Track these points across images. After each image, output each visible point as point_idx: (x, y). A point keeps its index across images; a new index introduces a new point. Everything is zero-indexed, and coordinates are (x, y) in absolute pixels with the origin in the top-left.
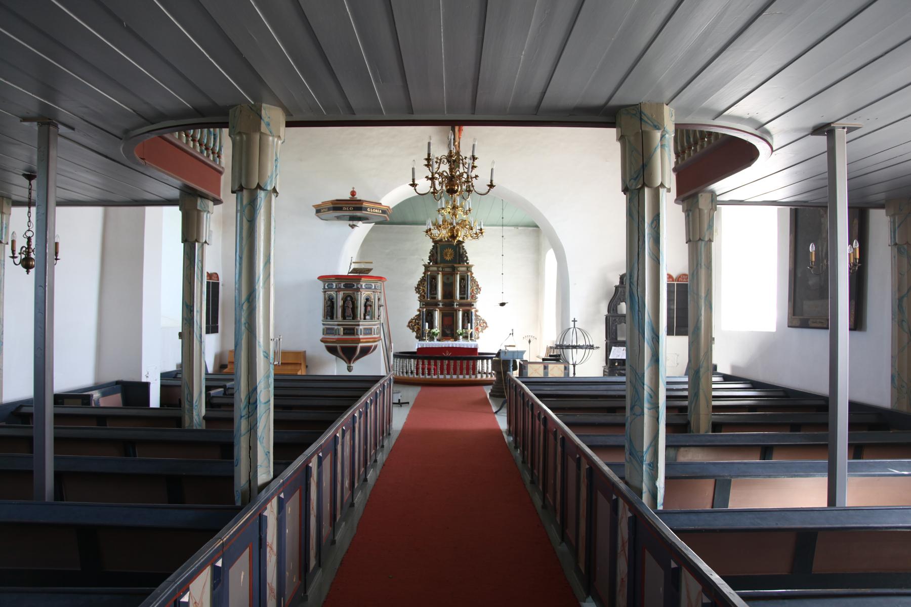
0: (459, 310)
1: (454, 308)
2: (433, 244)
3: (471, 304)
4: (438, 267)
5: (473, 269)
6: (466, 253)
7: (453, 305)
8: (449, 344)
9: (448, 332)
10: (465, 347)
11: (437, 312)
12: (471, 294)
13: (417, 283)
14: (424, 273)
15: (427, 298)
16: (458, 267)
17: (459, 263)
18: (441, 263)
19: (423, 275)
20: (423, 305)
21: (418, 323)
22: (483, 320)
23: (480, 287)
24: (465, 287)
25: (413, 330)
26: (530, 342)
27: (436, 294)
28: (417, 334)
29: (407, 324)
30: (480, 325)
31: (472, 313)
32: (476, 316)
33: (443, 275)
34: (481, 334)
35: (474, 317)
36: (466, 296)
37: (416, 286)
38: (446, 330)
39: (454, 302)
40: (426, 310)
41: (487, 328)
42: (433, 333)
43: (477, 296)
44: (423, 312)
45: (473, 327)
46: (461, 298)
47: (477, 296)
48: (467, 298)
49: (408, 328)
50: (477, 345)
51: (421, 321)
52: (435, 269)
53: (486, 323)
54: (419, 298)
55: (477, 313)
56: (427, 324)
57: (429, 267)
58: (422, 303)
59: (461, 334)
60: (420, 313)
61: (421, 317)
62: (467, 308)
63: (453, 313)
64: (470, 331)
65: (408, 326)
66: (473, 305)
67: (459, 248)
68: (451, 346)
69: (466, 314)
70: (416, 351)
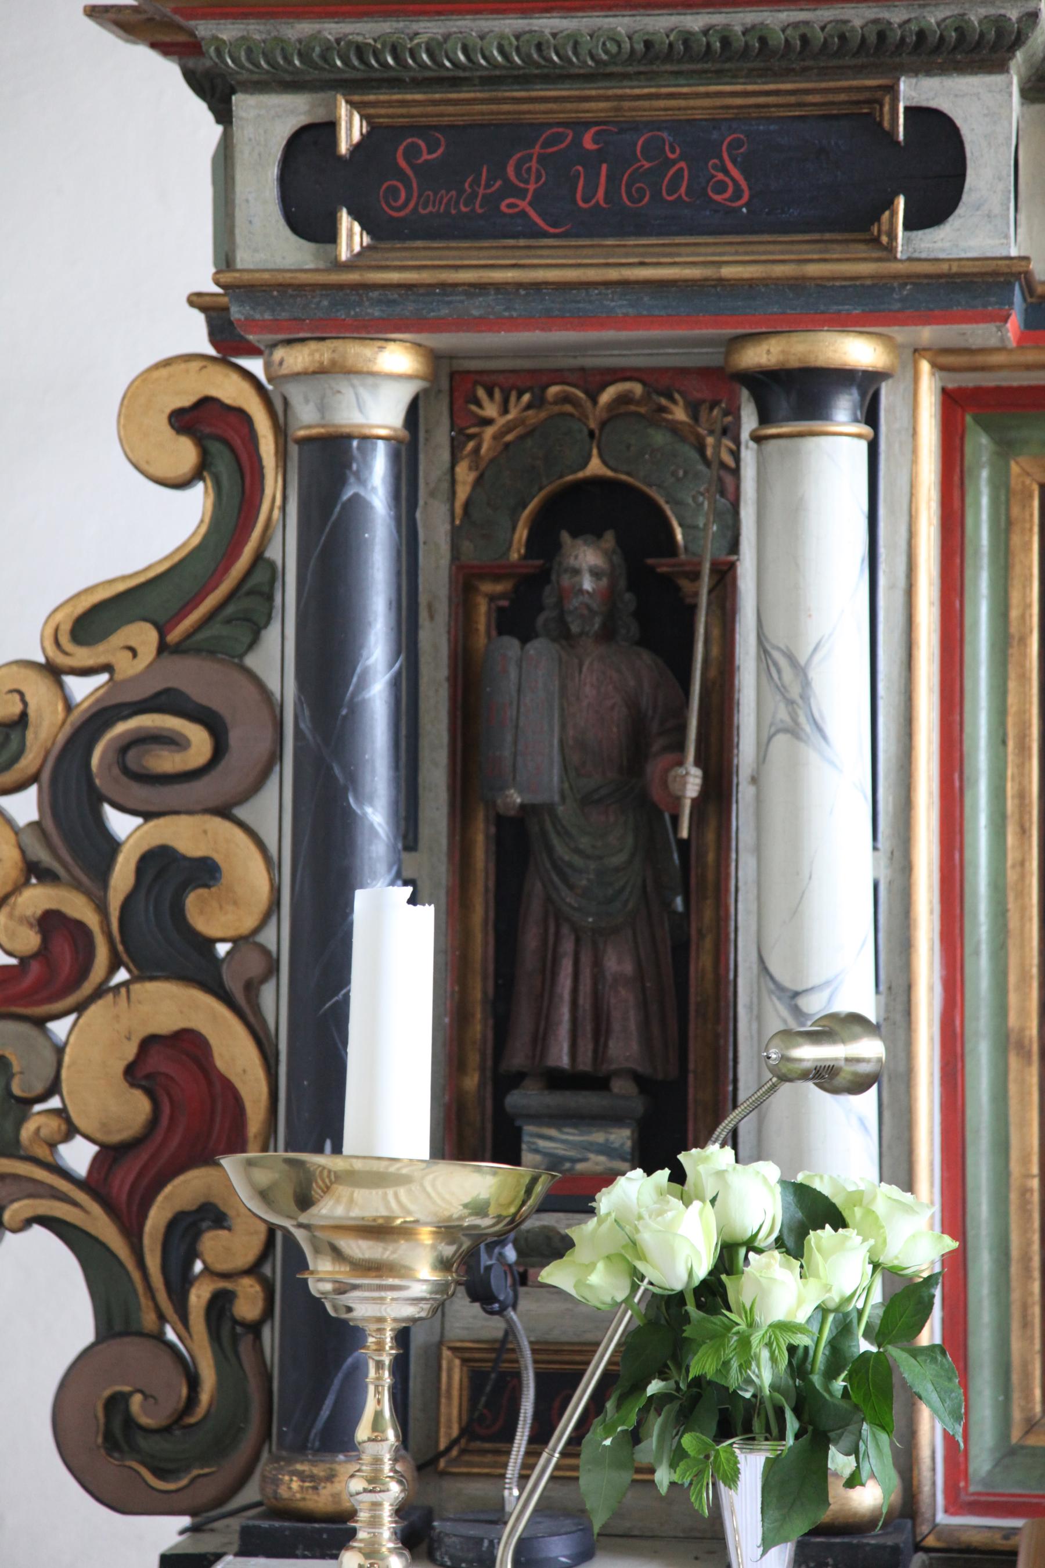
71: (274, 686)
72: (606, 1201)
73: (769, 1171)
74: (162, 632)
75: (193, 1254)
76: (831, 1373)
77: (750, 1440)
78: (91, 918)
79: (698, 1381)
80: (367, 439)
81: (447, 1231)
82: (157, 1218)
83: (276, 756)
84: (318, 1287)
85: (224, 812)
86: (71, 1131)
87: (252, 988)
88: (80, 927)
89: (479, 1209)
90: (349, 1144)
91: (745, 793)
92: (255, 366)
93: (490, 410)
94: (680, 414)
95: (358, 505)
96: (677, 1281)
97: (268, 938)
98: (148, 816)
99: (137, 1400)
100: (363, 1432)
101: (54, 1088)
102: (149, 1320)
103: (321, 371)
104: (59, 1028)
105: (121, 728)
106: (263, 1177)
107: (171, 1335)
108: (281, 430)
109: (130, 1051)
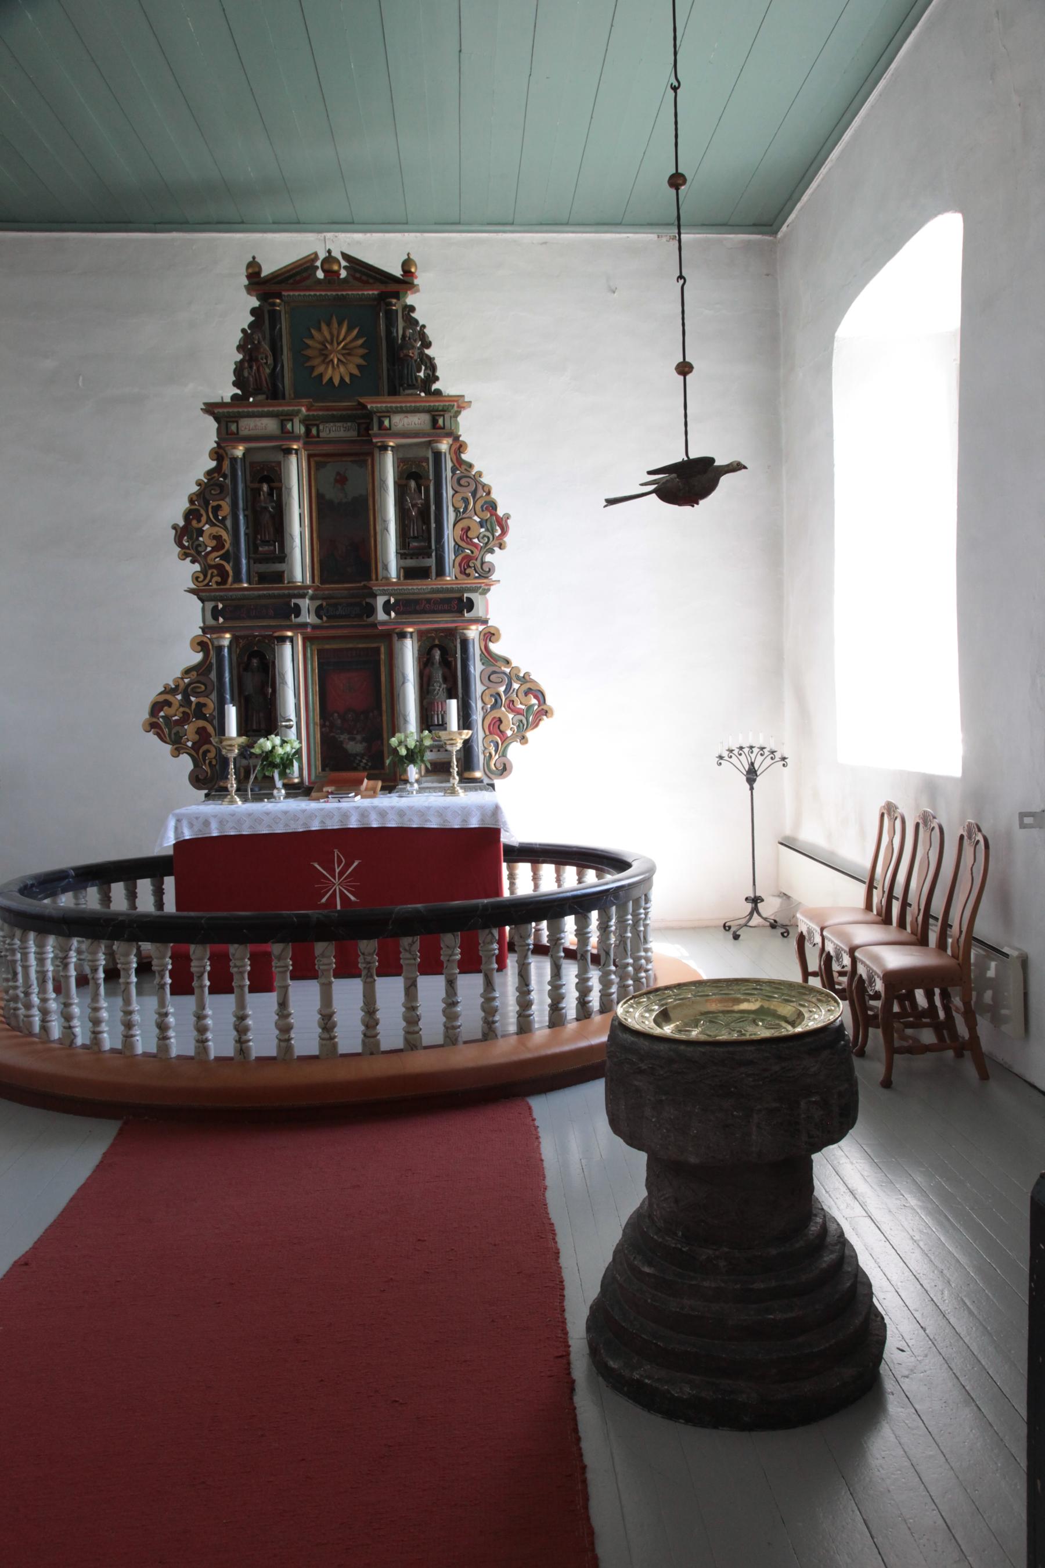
0: (402, 635)
1: (374, 625)
2: (255, 302)
3: (460, 599)
4: (284, 418)
5: (467, 425)
6: (428, 345)
7: (371, 610)
8: (345, 815)
9: (354, 747)
10: (434, 824)
11: (287, 648)
12: (458, 549)
13: (186, 505)
14: (218, 454)
15: (238, 579)
16: (389, 412)
17: (393, 392)
18: (298, 395)
19: (213, 464)
20: (215, 613)
21: (200, 706)
22: (525, 679)
23: (500, 512)
24: (424, 513)
25: (178, 746)
26: (752, 775)
27: (282, 556)
28: (196, 764)
29: (145, 715)
30: (511, 706)
31: (465, 642)
32: (489, 657)
33: (317, 463)
34: (515, 751)
35: (477, 668)
36: (432, 562)
37: (181, 523)
38: (344, 737)
39: (374, 596)
40: (235, 640)
41: (545, 722)
42: (268, 756)
43: (489, 558)
44: (220, 649)
45: (478, 716)
46: (409, 573)
47: (489, 558)
48: (441, 572)
49: (152, 738)
50: (496, 810)
51: (214, 696)
52: (269, 425)
53: (540, 695)
54: (196, 578)
55: (494, 647)
56: (232, 712)
57: (236, 418)
58: (210, 605)
59: (412, 756)
60: (206, 655)
61: (213, 675)
62: (443, 621)
63: (377, 650)
64: (455, 736)
65: (152, 726)
66: (470, 605)
67: (391, 317)
68: (353, 824)
69: (437, 654)
70: (171, 852)
71: (213, 679)
72: (259, 742)
73: (279, 738)
74: (197, 672)
75: (206, 756)
76: (287, 760)
77: (277, 768)
78: (189, 712)
79: (270, 762)
80: (224, 646)
81: (239, 746)
82: (201, 751)
83: (214, 689)
84: (224, 753)
85: (207, 697)
86: (188, 741)
87: (212, 720)
88: (187, 713)
89: (242, 743)
90: (226, 735)
91: (278, 692)
92: (209, 636)
93: (241, 641)
94: (267, 641)
95: (224, 655)
96: (267, 750)
97: (214, 714)
98: (196, 698)
99: (200, 776)
100: (230, 770)
101: (186, 735)
102: (200, 765)
103: (217, 638)
104: (186, 727)
105: (192, 686)
106: (217, 740)
107: (204, 767)
108: (213, 645)
109: (196, 729)
